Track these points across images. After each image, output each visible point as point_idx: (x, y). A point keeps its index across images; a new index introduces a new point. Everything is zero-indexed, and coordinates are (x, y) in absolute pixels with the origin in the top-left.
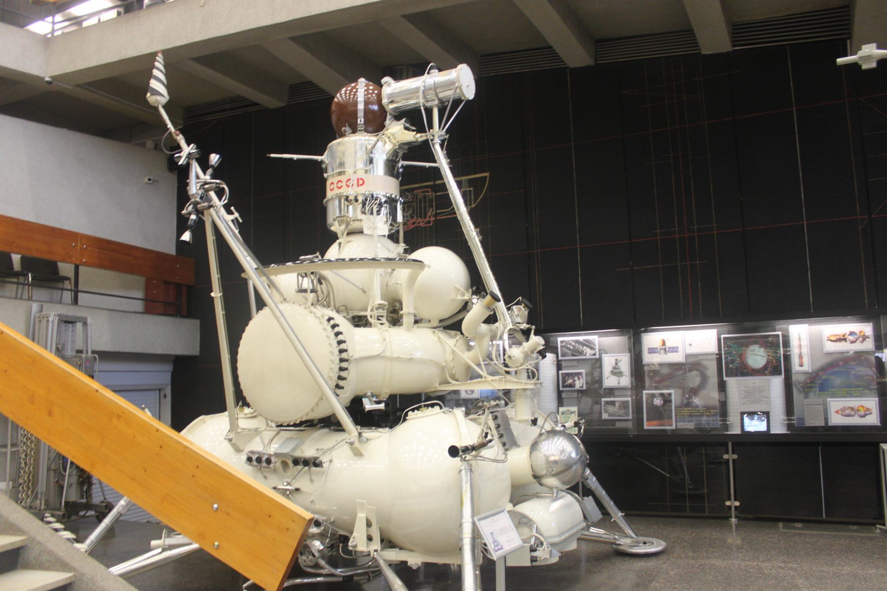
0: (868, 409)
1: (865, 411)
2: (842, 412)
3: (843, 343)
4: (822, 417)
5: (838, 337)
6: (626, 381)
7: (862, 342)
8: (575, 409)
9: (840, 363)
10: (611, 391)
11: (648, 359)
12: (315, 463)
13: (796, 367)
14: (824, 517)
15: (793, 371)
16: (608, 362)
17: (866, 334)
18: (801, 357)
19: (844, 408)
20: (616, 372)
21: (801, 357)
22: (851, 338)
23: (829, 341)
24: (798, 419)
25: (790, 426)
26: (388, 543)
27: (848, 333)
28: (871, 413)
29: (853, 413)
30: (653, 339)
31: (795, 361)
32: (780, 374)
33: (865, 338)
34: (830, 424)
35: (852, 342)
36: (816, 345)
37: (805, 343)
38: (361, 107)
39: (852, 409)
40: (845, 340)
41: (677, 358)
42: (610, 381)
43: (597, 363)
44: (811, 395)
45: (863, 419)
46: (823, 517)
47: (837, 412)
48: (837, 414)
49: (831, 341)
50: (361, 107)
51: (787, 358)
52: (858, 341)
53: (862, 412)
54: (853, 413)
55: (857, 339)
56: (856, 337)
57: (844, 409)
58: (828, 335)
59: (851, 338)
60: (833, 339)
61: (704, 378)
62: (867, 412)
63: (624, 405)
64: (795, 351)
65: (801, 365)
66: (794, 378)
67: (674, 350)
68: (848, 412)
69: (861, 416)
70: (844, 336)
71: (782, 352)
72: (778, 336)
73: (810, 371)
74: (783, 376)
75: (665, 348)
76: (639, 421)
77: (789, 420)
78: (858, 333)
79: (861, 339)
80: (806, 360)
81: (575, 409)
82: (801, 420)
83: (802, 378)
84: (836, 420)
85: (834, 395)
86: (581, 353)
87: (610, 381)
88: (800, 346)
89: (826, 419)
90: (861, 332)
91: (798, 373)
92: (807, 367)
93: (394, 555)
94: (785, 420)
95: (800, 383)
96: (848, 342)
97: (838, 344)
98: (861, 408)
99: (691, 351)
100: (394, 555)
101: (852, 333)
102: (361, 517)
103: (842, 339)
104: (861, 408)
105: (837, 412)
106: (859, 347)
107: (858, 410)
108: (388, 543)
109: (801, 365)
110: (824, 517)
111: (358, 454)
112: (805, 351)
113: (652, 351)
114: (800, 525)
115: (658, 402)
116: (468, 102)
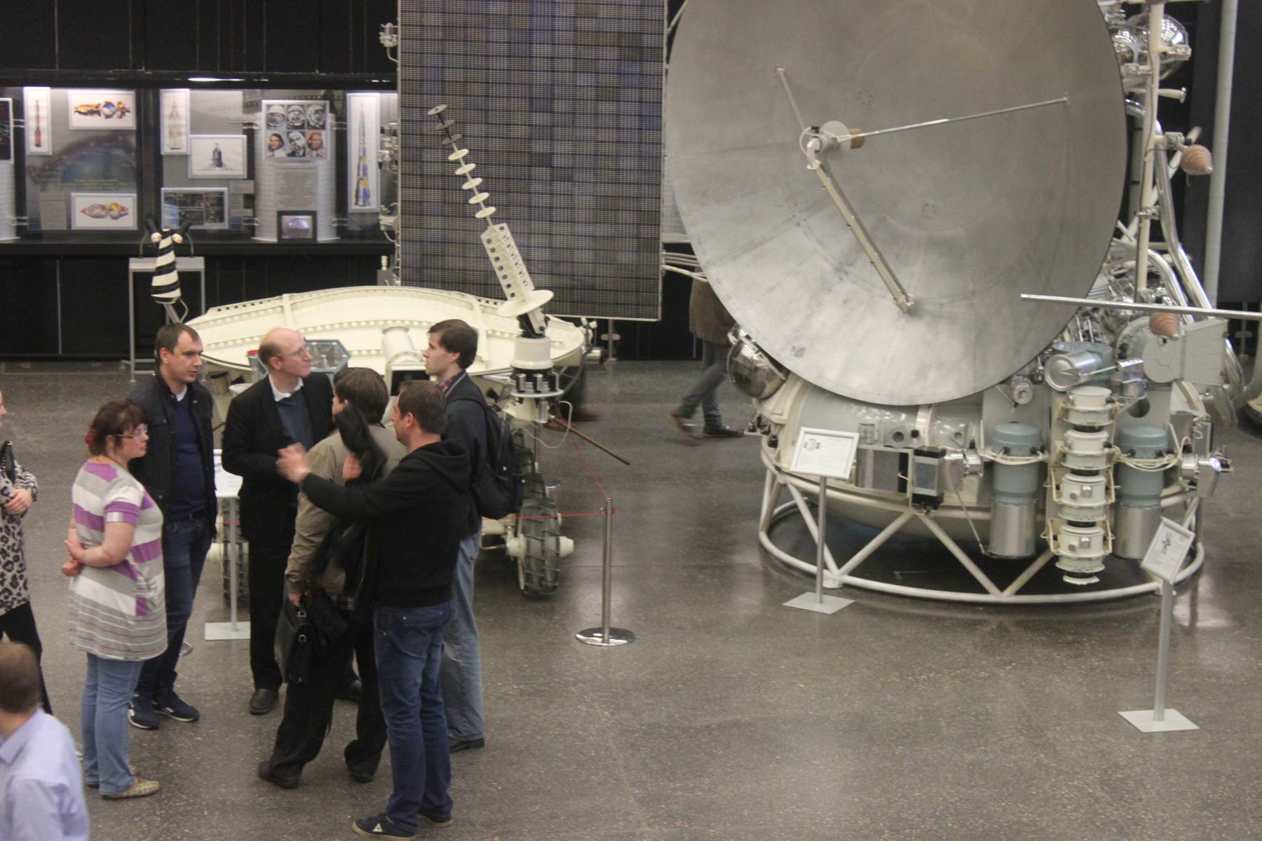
0: (123, 209)
1: (119, 211)
2: (90, 212)
3: (96, 117)
4: (64, 219)
5: (89, 109)
7: (121, 117)
9: (91, 144)
13: (31, 148)
14: (60, 352)
15: (27, 153)
17: (126, 107)
18: (38, 132)
19: (93, 206)
21: (38, 132)
22: (107, 111)
23: (77, 114)
24: (31, 220)
25: (19, 230)
27: (103, 104)
28: (126, 214)
29: (103, 213)
31: (30, 138)
32: (8, 158)
33: (124, 111)
34: (73, 228)
35: (108, 117)
36: (60, 115)
37: (45, 113)
39: (103, 207)
40: (98, 113)
44: (50, 186)
45: (115, 221)
46: (57, 351)
47: (83, 211)
48: (82, 214)
49: (81, 113)
51: (20, 134)
52: (115, 116)
53: (115, 213)
54: (103, 213)
55: (114, 113)
56: (113, 109)
57: (92, 208)
58: (77, 106)
59: (107, 111)
60: (83, 110)
62: (123, 212)
64: (30, 124)
65: (38, 145)
66: (28, 162)
68: (98, 211)
69: (115, 218)
70: (97, 107)
71: (12, 126)
72: (7, 103)
73: (50, 154)
74: (12, 161)
77: (19, 221)
78: (115, 103)
79: (119, 113)
80: (45, 138)
82: (36, 221)
83: (38, 163)
84: (82, 222)
85: (80, 188)
88: (38, 118)
89: (69, 221)
90: (120, 103)
91: (34, 156)
92: (46, 148)
94: (13, 221)
95: (35, 169)
96: (103, 116)
97: (88, 118)
98: (114, 207)
101: (108, 105)
103: (94, 111)
104: (114, 207)
105: (83, 211)
106: (115, 123)
107: (111, 210)
109: (38, 145)
110: (60, 352)
112: (45, 124)
114: (27, 365)
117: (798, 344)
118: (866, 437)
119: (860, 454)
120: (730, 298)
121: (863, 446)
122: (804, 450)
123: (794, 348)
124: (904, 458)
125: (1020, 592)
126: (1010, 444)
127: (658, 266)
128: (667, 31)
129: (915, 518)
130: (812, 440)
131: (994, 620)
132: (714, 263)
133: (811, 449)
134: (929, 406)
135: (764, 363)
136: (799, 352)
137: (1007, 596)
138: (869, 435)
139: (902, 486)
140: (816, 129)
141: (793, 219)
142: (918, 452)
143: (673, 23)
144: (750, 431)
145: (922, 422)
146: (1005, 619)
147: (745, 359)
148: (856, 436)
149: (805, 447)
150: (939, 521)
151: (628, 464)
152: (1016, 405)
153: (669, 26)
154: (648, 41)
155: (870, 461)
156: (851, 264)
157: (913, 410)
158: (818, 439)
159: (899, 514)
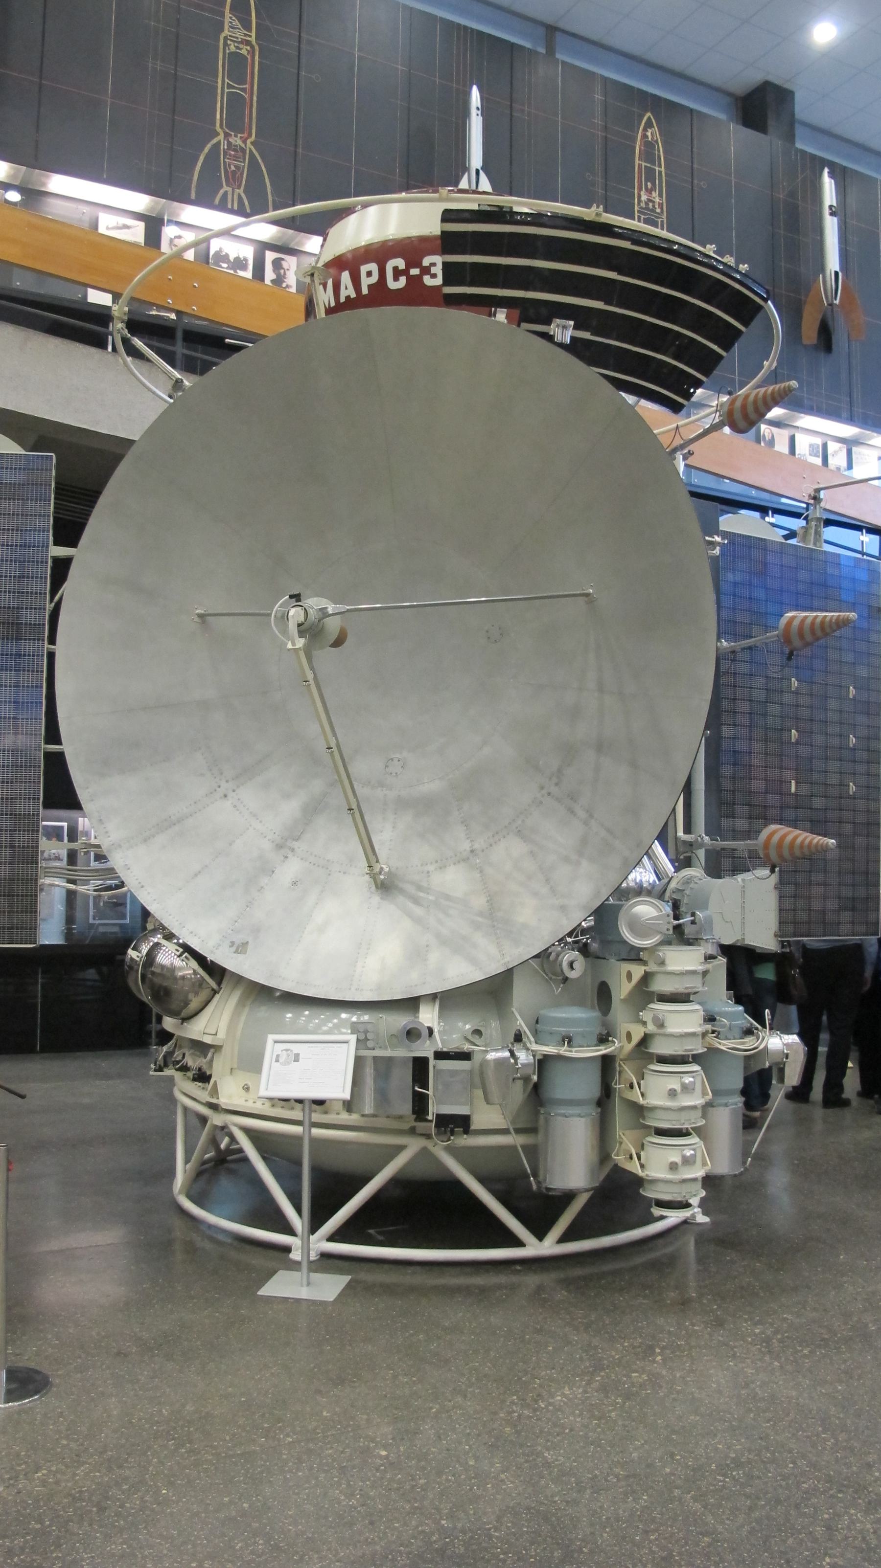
117: (239, 938)
118: (366, 1039)
119: (359, 1062)
120: (142, 887)
121: (364, 1053)
122: (275, 1064)
123: (233, 943)
124: (420, 1066)
125: (564, 1239)
126: (572, 1030)
127: (36, 880)
128: (49, 607)
129: (424, 1151)
130: (287, 1050)
131: (532, 1280)
132: (120, 846)
133: (287, 1063)
134: (434, 997)
135: (187, 968)
136: (241, 948)
137: (548, 1246)
138: (370, 1036)
139: (420, 1104)
140: (297, 597)
141: (218, 789)
142: (440, 1055)
143: (57, 598)
144: (156, 1070)
145: (428, 1016)
146: (547, 1278)
147: (163, 967)
148: (353, 1038)
149: (277, 1061)
150: (461, 1155)
151: (23, 1097)
152: (566, 980)
153: (51, 600)
154: (27, 617)
155: (369, 1071)
156: (297, 839)
157: (412, 1004)
158: (296, 1048)
159: (401, 1148)
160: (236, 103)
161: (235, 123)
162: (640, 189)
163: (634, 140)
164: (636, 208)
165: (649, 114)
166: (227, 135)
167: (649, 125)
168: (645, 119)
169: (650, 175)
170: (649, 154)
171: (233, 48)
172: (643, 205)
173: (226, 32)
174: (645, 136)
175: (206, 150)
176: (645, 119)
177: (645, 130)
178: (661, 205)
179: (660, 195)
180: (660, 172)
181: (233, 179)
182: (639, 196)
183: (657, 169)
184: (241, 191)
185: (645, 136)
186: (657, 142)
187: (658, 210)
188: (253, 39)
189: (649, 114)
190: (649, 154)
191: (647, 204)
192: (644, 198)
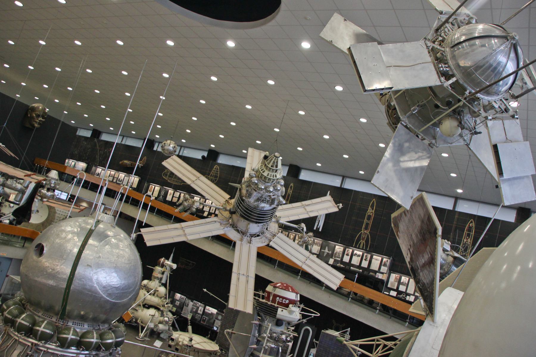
6: (201, 313)
8: (192, 314)
10: (199, 314)
11: (206, 310)
12: (137, 310)
16: (200, 308)
20: (201, 311)
26: (142, 322)
30: (207, 307)
38: (161, 263)
41: (210, 312)
42: (199, 312)
43: (198, 308)
50: (161, 263)
61: (213, 318)
63: (199, 317)
67: (210, 311)
75: (209, 310)
76: (200, 320)
81: (192, 314)
86: (197, 305)
87: (199, 312)
93: (142, 324)
99: (212, 312)
100: (142, 324)
102: (140, 318)
108: (142, 322)
111: (142, 311)
113: (207, 309)
115: (204, 319)
116: (174, 270)
160: (367, 224)
161: (366, 228)
162: (464, 238)
163: (465, 227)
164: (462, 243)
165: (472, 220)
166: (364, 231)
167: (472, 222)
168: (470, 221)
169: (468, 235)
170: (470, 229)
171: (369, 214)
172: (464, 242)
173: (368, 211)
174: (469, 225)
175: (359, 233)
176: (470, 221)
177: (470, 224)
178: (470, 242)
179: (471, 240)
180: (472, 234)
181: (363, 239)
182: (464, 240)
183: (471, 233)
184: (364, 241)
185: (469, 225)
186: (473, 226)
187: (469, 244)
188: (373, 212)
189: (472, 220)
190: (470, 229)
191: (466, 242)
192: (465, 240)
